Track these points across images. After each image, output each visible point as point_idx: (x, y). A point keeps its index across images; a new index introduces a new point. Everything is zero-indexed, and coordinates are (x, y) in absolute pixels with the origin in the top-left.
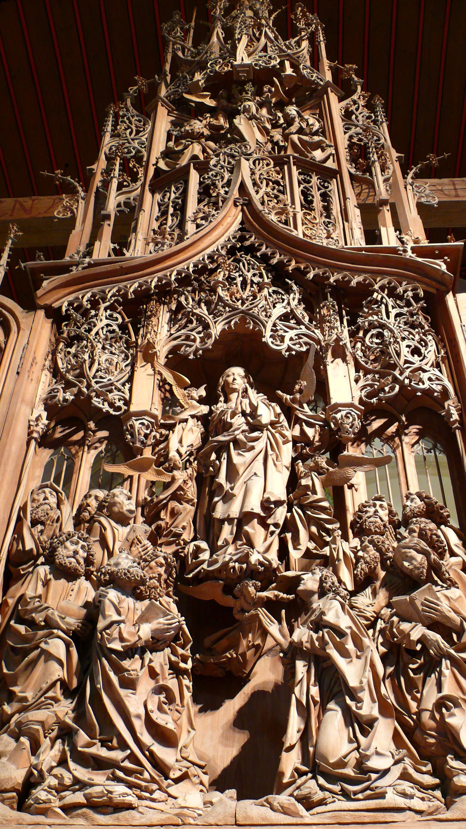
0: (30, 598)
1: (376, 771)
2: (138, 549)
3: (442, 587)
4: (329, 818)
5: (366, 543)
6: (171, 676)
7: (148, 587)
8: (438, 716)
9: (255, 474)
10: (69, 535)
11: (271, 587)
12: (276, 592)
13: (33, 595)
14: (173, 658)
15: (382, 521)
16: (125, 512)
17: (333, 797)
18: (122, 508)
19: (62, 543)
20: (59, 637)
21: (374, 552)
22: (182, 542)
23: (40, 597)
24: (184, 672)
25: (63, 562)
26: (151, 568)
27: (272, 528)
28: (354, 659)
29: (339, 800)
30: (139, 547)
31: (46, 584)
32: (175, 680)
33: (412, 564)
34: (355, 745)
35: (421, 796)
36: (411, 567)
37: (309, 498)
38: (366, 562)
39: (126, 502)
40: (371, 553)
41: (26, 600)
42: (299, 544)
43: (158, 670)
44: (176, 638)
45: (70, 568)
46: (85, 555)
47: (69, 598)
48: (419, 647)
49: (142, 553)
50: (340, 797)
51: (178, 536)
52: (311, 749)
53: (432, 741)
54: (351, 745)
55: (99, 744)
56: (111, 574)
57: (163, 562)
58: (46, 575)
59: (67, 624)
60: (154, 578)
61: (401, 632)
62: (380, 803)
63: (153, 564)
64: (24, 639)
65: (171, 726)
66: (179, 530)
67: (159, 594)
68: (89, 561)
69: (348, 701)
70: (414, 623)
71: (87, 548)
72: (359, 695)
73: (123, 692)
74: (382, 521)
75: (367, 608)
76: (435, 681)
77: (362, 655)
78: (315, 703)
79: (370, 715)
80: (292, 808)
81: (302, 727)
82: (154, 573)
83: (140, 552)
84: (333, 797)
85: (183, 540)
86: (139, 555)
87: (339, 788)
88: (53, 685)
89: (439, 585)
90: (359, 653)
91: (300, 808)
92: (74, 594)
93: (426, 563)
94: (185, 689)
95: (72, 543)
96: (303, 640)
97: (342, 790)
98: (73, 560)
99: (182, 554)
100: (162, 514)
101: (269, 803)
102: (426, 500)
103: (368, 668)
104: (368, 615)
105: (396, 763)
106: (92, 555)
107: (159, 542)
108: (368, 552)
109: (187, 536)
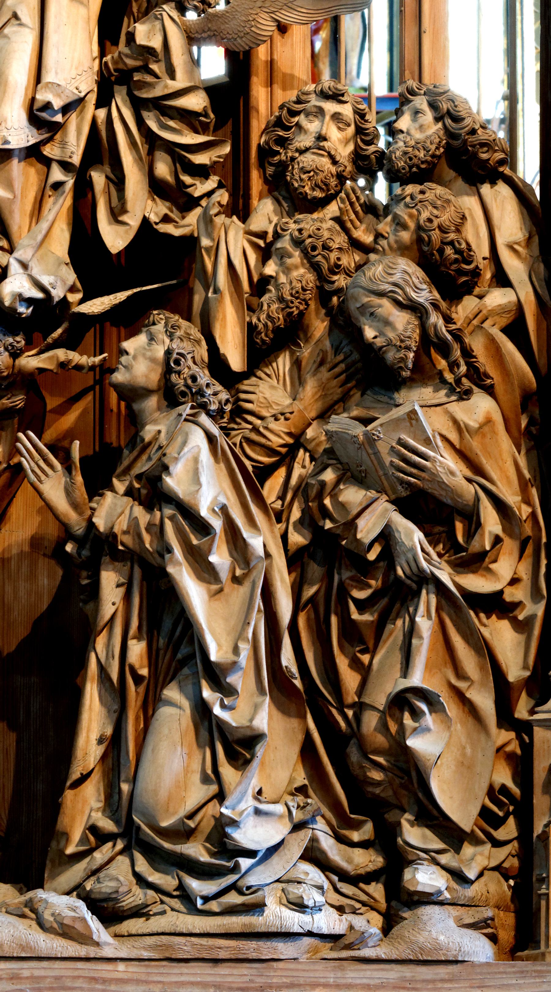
1: (250, 854)
3: (452, 391)
4: (151, 948)
5: (285, 243)
8: (393, 727)
9: (15, 16)
11: (49, 340)
12: (61, 354)
15: (335, 162)
17: (162, 902)
21: (302, 271)
27: (57, 174)
28: (228, 586)
29: (173, 909)
33: (382, 333)
34: (214, 789)
35: (337, 904)
36: (379, 342)
37: (150, 86)
38: (281, 299)
40: (295, 274)
42: (124, 211)
48: (372, 556)
50: (176, 903)
52: (125, 787)
53: (376, 775)
54: (206, 787)
61: (342, 507)
62: (251, 924)
69: (207, 693)
70: (372, 494)
72: (229, 680)
74: (335, 162)
75: (273, 425)
76: (401, 638)
77: (245, 576)
78: (138, 679)
79: (250, 727)
80: (78, 926)
81: (109, 731)
84: (162, 902)
87: (175, 883)
89: (443, 381)
90: (238, 572)
91: (94, 923)
93: (416, 336)
96: (116, 530)
97: (181, 887)
101: (33, 910)
102: (448, 121)
103: (258, 602)
104: (275, 441)
105: (298, 827)
108: (287, 270)
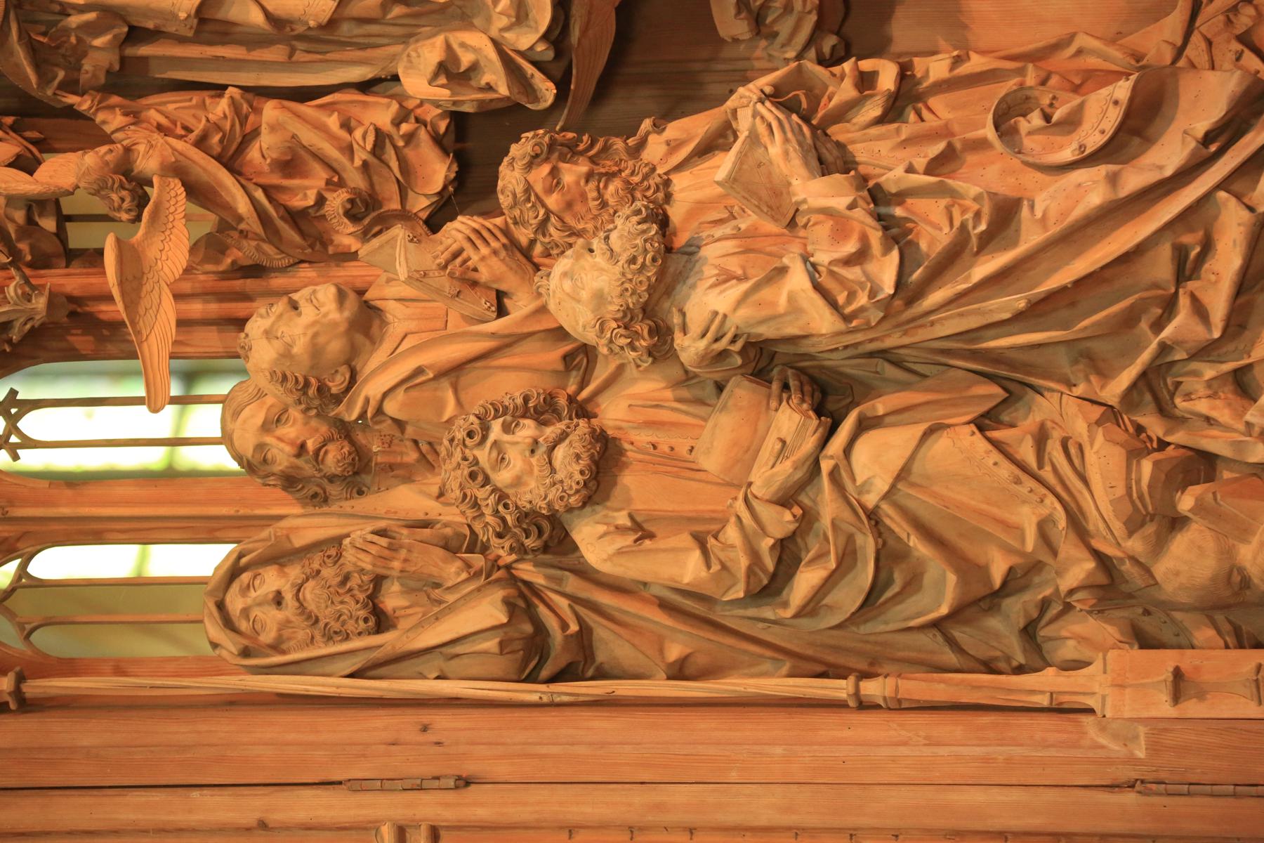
0: (709, 567)
2: (483, 259)
6: (925, 114)
10: (473, 476)
13: (695, 558)
14: (873, 110)
16: (347, 314)
18: (334, 324)
19: (502, 497)
20: (848, 450)
22: (405, 127)
23: (700, 541)
24: (905, 74)
26: (569, 205)
30: (475, 258)
31: (641, 530)
32: (933, 102)
39: (308, 313)
41: (716, 578)
43: (938, 148)
44: (789, 107)
46: (528, 422)
47: (683, 450)
49: (495, 244)
51: (380, 136)
56: (626, 320)
57: (545, 169)
58: (620, 530)
59: (800, 432)
60: (600, 195)
63: (553, 201)
64: (848, 558)
65: (1123, 90)
66: (363, 141)
67: (646, 177)
68: (543, 411)
73: (1030, 237)
82: (583, 196)
85: (397, 123)
86: (503, 254)
88: (997, 445)
94: (964, 69)
99: (443, 126)
100: (298, 202)
106: (526, 399)
109: (381, 113)
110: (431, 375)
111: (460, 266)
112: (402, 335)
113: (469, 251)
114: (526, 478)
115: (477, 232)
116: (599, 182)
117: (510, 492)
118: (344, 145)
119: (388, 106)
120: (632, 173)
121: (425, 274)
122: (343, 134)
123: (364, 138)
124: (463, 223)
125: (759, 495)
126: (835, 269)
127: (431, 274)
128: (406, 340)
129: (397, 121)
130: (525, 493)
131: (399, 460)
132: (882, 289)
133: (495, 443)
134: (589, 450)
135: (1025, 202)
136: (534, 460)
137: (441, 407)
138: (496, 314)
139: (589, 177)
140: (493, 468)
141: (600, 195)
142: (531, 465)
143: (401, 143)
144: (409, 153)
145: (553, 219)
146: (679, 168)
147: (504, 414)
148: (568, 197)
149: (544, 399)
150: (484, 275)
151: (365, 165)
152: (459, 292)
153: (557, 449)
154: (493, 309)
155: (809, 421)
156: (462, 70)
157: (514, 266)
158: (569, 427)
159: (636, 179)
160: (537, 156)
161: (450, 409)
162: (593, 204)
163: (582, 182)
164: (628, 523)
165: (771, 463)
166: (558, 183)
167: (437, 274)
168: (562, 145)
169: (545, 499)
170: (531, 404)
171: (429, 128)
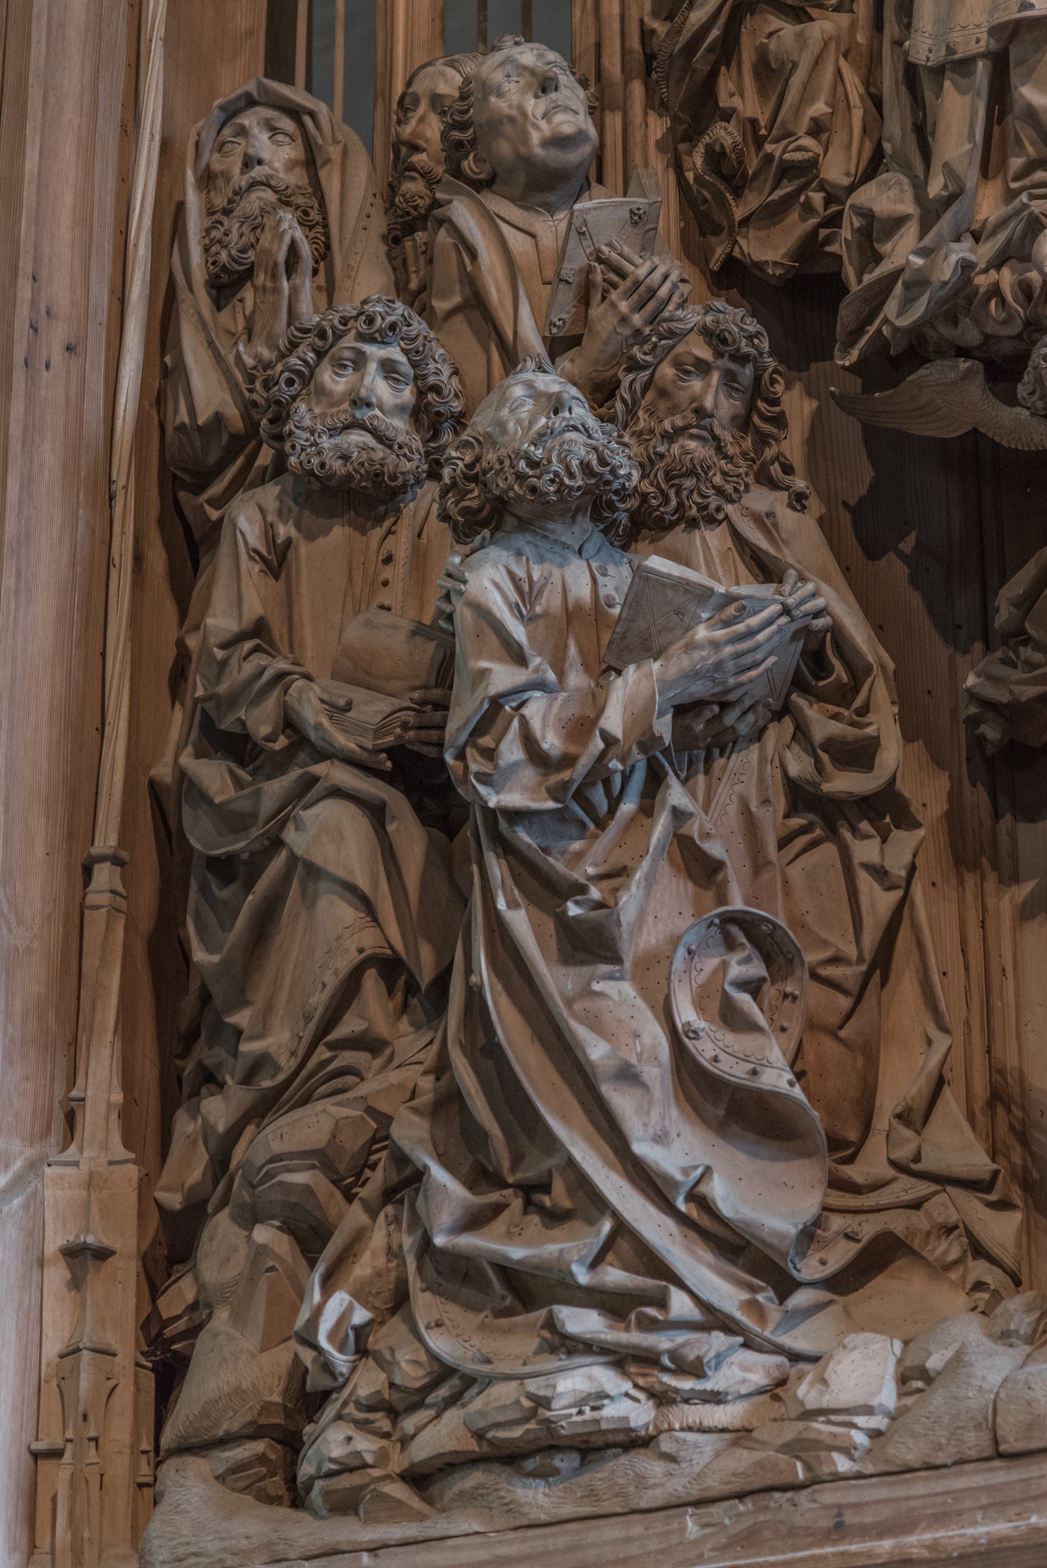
2: (614, 306)
7: (668, 476)
10: (322, 335)
20: (337, 792)
22: (817, 198)
25: (315, 461)
26: (663, 393)
45: (349, 477)
49: (637, 319)
55: (517, 1203)
57: (704, 353)
58: (269, 532)
60: (679, 432)
71: (406, 368)
82: (673, 410)
83: (624, 320)
86: (626, 332)
92: (398, 573)
95: (340, 365)
98: (356, 438)
106: (436, 389)
107: (739, 213)
110: (469, 268)
111: (605, 280)
112: (533, 231)
113: (624, 285)
114: (325, 400)
115: (653, 292)
116: (698, 427)
117: (312, 385)
118: (790, 127)
119: (848, 174)
120: (724, 474)
121: (583, 234)
122: (805, 123)
123: (799, 149)
124: (666, 277)
125: (291, 691)
126: (515, 723)
127: (586, 243)
128: (528, 238)
129: (828, 188)
130: (309, 403)
131: (412, 269)
132: (498, 793)
133: (361, 353)
134: (357, 472)
135: (617, 968)
136: (346, 406)
137: (444, 296)
138: (547, 334)
139: (700, 412)
140: (332, 357)
141: (679, 432)
142: (340, 402)
143: (802, 198)
144: (794, 215)
145: (644, 375)
146: (736, 535)
147: (414, 365)
148: (670, 387)
149: (439, 414)
150: (596, 311)
151: (769, 158)
152: (567, 282)
153: (363, 432)
154: (554, 330)
155: (371, 736)
156: (876, 245)
157: (611, 349)
158: (400, 447)
159: (718, 480)
160: (724, 341)
161: (441, 305)
162: (667, 425)
163: (694, 405)
164: (279, 541)
165: (326, 697)
166: (688, 373)
167: (588, 251)
168: (757, 379)
169: (297, 427)
170: (431, 397)
171: (827, 231)
